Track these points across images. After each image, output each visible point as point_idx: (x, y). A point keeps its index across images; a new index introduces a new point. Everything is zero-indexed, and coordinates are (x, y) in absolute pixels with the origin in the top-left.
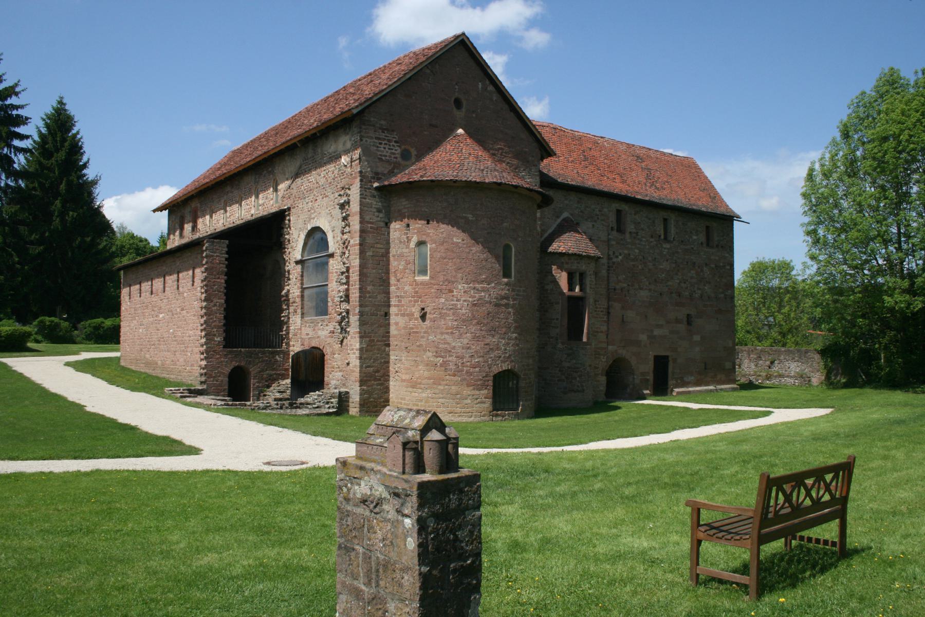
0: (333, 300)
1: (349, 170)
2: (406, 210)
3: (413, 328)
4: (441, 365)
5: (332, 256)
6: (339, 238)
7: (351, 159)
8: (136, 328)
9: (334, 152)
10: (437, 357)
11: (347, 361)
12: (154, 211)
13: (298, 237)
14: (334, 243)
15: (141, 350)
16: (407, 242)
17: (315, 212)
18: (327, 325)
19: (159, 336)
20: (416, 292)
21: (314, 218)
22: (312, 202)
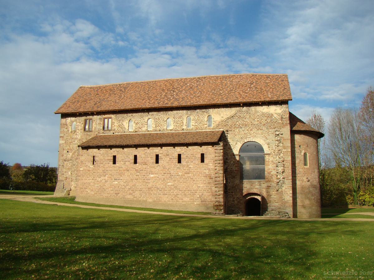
0: (269, 173)
1: (280, 121)
2: (299, 140)
3: (304, 185)
4: (314, 199)
5: (269, 154)
6: (274, 148)
7: (282, 117)
8: (106, 181)
9: (267, 112)
10: (312, 196)
11: (283, 198)
12: (55, 113)
13: (236, 144)
14: (269, 150)
15: (117, 194)
16: (300, 152)
17: (250, 135)
18: (263, 183)
19: (150, 185)
20: (304, 172)
21: (250, 137)
22: (247, 130)
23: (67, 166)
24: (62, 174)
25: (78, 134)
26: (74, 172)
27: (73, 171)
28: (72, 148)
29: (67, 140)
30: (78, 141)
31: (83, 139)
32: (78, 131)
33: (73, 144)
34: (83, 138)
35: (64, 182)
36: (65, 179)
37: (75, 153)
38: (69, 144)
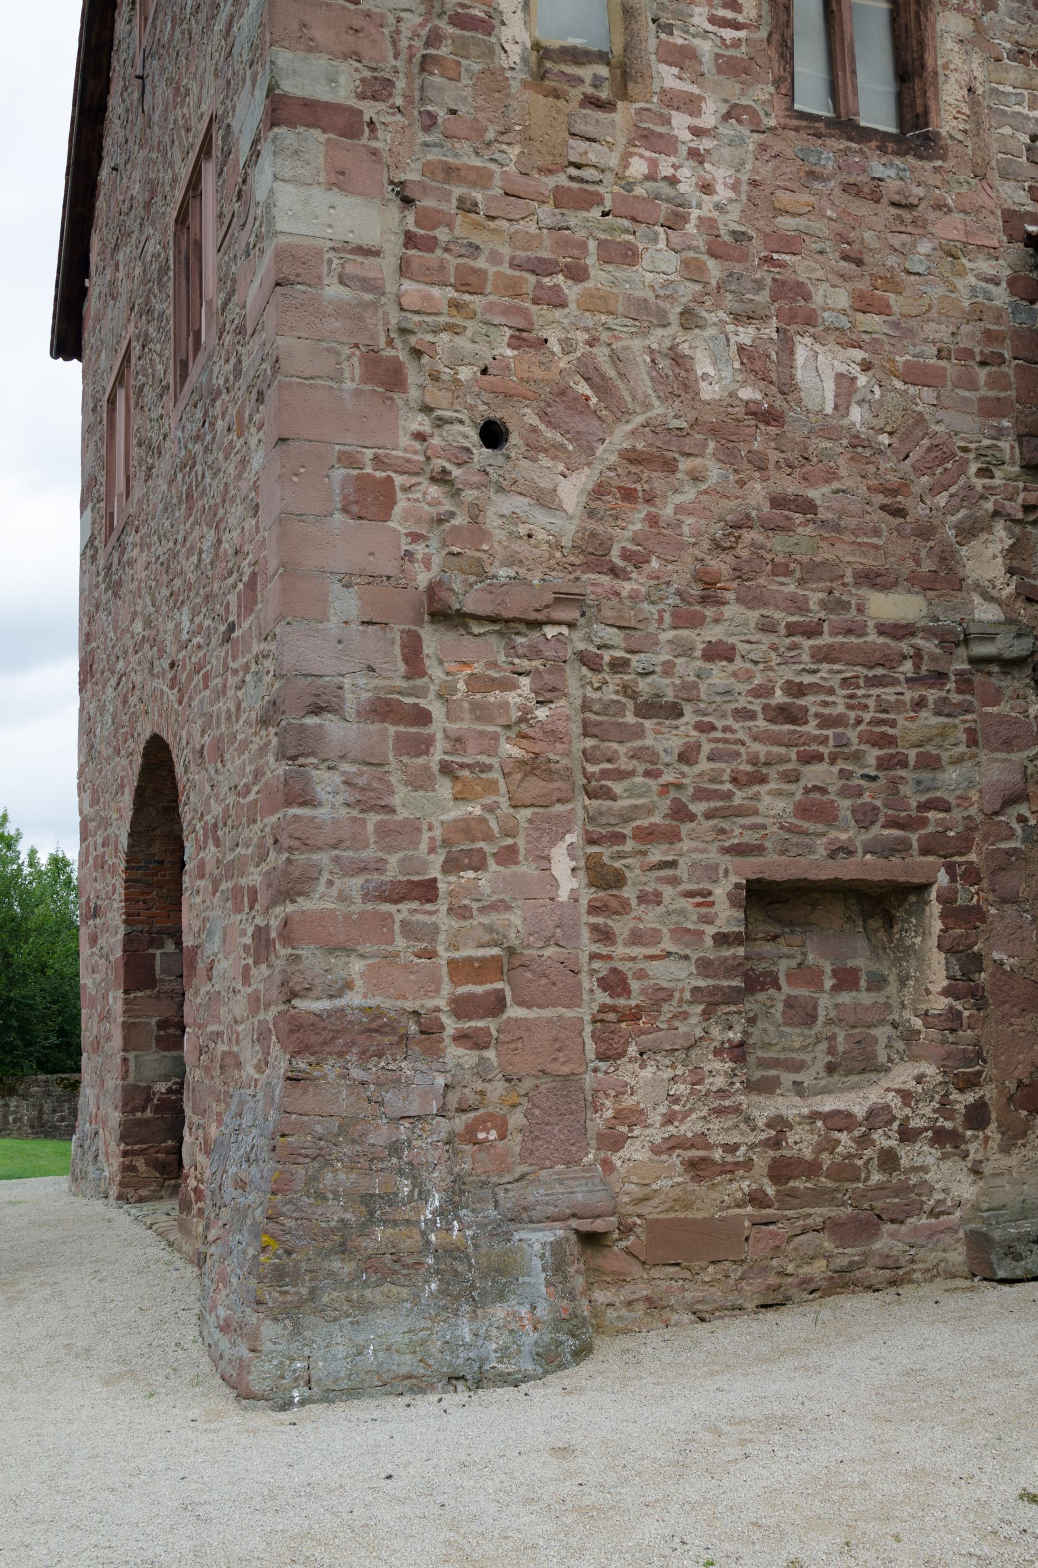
23: (482, 714)
24: (398, 894)
25: (680, 123)
26: (657, 854)
27: (648, 835)
28: (602, 386)
29: (468, 207)
30: (692, 270)
31: (791, 244)
32: (668, 77)
33: (592, 304)
34: (786, 222)
35: (455, 1053)
36: (461, 1008)
37: (658, 481)
38: (513, 289)
